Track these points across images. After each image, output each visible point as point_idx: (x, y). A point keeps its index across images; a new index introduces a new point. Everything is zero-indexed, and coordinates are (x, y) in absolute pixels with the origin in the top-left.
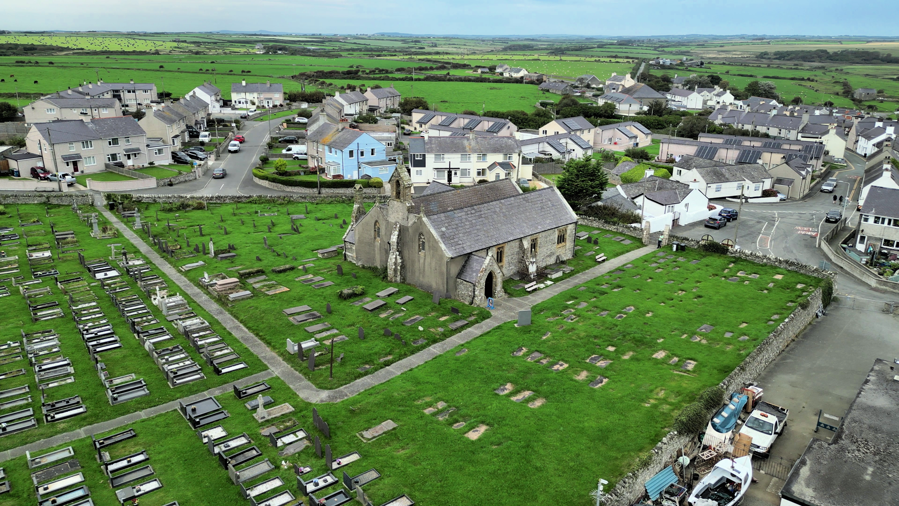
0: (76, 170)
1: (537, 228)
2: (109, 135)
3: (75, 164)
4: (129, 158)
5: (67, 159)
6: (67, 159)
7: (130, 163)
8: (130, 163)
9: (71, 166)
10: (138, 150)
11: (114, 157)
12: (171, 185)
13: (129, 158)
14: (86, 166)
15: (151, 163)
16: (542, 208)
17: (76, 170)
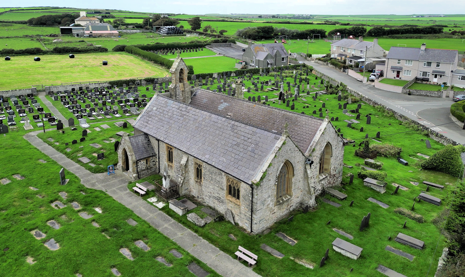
0: (398, 76)
1: (204, 155)
2: (425, 60)
3: (398, 73)
4: (436, 77)
5: (393, 68)
6: (393, 68)
7: (435, 80)
8: (435, 80)
9: (395, 74)
10: (444, 72)
11: (425, 73)
12: (409, 94)
13: (436, 77)
14: (404, 76)
15: (444, 83)
16: (238, 145)
17: (398, 76)
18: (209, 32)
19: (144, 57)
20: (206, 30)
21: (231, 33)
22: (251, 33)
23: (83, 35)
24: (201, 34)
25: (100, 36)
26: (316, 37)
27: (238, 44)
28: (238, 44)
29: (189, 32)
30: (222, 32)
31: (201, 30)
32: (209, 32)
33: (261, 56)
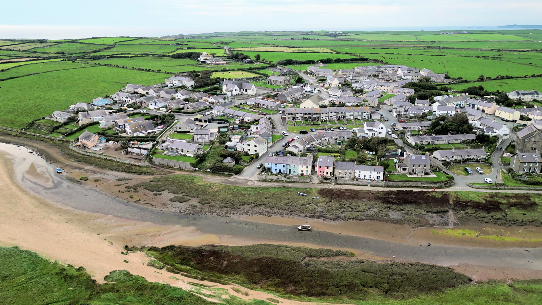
18: (264, 61)
19: (251, 72)
20: (263, 60)
21: (275, 62)
22: (283, 62)
23: (212, 64)
24: (261, 62)
25: (219, 64)
26: (310, 63)
27: (278, 67)
28: (278, 67)
29: (256, 62)
30: (270, 62)
31: (261, 60)
32: (264, 61)
33: (285, 71)
